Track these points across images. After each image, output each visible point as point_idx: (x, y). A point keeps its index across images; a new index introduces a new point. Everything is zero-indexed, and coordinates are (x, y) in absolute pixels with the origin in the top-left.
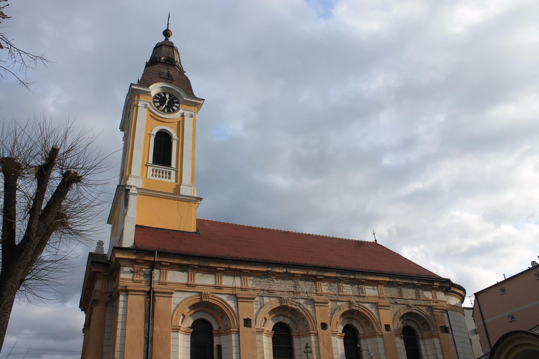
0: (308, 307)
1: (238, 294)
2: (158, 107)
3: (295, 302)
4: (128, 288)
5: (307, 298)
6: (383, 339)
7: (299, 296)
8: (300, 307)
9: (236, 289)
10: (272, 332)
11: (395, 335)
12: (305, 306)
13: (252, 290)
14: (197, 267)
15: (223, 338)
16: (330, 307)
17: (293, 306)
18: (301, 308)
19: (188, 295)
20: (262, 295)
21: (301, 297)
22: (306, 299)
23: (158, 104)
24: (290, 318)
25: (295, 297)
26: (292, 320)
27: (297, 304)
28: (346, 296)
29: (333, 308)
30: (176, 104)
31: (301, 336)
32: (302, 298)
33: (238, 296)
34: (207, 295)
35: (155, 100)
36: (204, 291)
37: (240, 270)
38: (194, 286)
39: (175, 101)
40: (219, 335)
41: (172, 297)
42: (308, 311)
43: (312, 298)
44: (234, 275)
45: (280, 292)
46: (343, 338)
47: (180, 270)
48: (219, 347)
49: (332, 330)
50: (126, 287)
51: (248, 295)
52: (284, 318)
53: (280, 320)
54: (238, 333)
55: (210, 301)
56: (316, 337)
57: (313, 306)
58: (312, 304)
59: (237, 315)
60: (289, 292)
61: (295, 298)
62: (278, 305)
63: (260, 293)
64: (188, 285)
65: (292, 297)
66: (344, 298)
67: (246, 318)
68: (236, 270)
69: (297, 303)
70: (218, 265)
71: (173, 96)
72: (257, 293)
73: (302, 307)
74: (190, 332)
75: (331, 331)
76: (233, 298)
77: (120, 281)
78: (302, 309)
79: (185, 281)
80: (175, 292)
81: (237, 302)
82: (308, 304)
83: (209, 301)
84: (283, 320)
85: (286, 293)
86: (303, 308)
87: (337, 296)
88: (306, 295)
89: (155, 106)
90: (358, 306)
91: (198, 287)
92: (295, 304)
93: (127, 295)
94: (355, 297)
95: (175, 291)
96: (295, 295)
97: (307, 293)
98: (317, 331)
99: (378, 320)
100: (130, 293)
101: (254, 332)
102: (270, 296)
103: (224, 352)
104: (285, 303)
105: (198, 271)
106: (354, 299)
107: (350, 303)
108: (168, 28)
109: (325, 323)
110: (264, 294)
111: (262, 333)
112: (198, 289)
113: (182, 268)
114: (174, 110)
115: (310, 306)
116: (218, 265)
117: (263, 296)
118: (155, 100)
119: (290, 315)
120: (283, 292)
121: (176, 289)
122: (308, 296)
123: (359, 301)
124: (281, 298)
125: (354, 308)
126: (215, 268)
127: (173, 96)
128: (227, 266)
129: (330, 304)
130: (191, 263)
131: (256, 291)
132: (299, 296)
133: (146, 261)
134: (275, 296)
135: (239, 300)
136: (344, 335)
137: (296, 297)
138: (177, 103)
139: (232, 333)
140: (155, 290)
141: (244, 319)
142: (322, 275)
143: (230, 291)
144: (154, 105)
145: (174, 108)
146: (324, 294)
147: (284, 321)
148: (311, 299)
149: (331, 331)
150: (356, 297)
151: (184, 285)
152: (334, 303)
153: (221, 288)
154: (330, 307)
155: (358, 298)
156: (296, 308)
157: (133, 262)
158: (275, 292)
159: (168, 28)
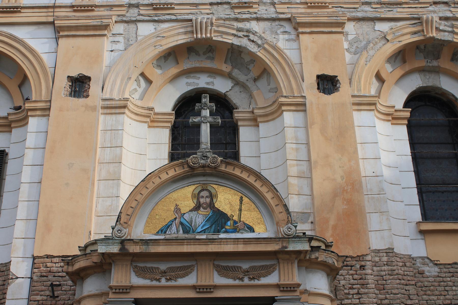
0: (278, 40)
3: (234, 29)
5: (274, 16)
7: (250, 13)
8: (250, 40)
9: (56, 10)
12: (269, 37)
13: (102, 9)
16: (350, 37)
17: (236, 41)
18: (253, 41)
20: (134, 19)
21: (254, 16)
22: (273, 20)
24: (229, 76)
25: (233, 16)
26: (237, 83)
27: (240, 34)
28: (404, 6)
29: (361, 38)
32: (258, 19)
42: (275, 48)
43: (289, 16)
45: (188, 7)
46: (406, 122)
49: (356, 93)
52: (210, 80)
53: (198, 84)
56: (301, 114)
57: (293, 37)
58: (293, 32)
60: (215, 7)
61: (237, 20)
62: (182, 39)
63: (128, 15)
65: (228, 16)
66: (399, 10)
67: (74, 74)
69: (239, 30)
72: (119, 16)
73: (255, 39)
75: (353, 96)
76: (48, 32)
78: (259, 46)
81: (57, 39)
82: (279, 32)
84: (208, 83)
85: (206, 9)
86: (260, 42)
87: (374, 6)
88: (273, 9)
90: (450, 29)
92: (234, 32)
94: (438, 6)
96: (237, 11)
97: (273, 4)
98: (304, 97)
101: (94, 109)
102: (156, 18)
104: (201, 34)
106: (434, 12)
107: (418, 20)
109: (331, 74)
110: (139, 15)
111: (122, 110)
115: (286, 36)
117: (136, 22)
119: (226, 68)
120: (196, 5)
122: (277, 12)
123: (450, 15)
124: (191, 20)
125: (434, 34)
129: (350, 27)
131: (115, 9)
132: (250, 13)
134: (173, 17)
136: (407, 115)
137: (239, 16)
141: (68, 77)
143: (41, 17)
146: (330, 3)
147: (210, 87)
148: (289, 20)
149: (353, 96)
150: (443, 5)
152: (366, 27)
154: (350, 37)
155: (447, 8)
156: (239, 44)
158: (173, 8)
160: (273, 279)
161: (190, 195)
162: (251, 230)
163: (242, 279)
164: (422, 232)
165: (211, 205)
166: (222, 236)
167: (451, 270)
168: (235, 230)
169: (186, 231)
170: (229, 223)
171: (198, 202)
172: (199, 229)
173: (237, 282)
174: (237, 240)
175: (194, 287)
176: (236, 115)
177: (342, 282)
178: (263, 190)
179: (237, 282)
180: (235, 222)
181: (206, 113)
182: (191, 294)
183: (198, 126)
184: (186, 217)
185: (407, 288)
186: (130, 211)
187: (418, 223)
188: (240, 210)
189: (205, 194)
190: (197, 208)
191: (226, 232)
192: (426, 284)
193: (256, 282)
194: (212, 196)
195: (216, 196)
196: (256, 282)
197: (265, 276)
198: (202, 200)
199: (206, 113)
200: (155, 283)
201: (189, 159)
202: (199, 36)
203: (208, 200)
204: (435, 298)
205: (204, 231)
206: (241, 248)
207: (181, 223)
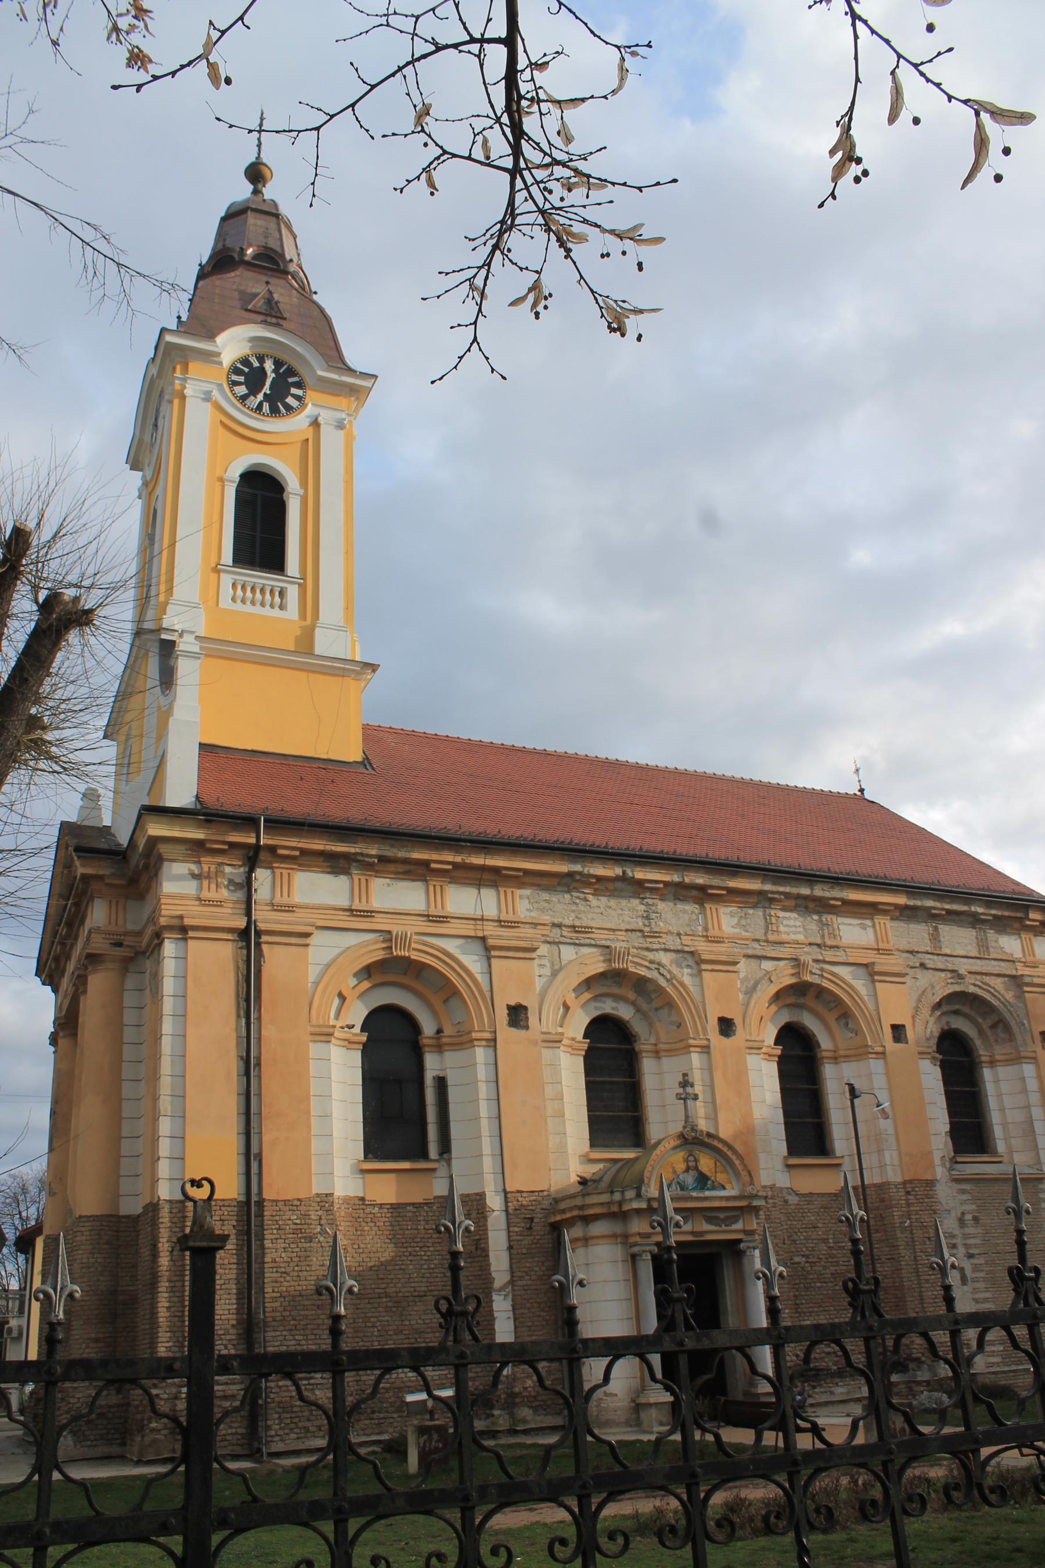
0: (683, 975)
1: (491, 935)
2: (243, 399)
3: (646, 960)
4: (187, 922)
5: (679, 948)
6: (886, 1063)
7: (659, 943)
8: (660, 973)
9: (485, 923)
10: (585, 1043)
11: (920, 1053)
12: (675, 970)
13: (527, 926)
14: (376, 861)
15: (451, 1058)
16: (742, 975)
17: (643, 972)
18: (663, 975)
19: (351, 939)
20: (557, 940)
21: (663, 946)
22: (677, 951)
23: (242, 390)
24: (633, 1004)
25: (645, 945)
26: (638, 1010)
27: (653, 966)
28: (786, 945)
29: (750, 976)
30: (294, 391)
31: (662, 1054)
32: (665, 950)
33: (491, 942)
35: (235, 378)
36: (395, 929)
37: (496, 870)
38: (369, 914)
39: (291, 380)
40: (439, 1048)
41: (307, 945)
42: (682, 984)
43: (692, 949)
44: (479, 884)
45: (606, 932)
46: (777, 1059)
47: (329, 870)
48: (441, 1083)
49: (748, 1038)
50: (181, 917)
51: (519, 938)
52: (614, 1005)
53: (604, 1009)
54: (492, 1044)
55: (415, 956)
56: (705, 1056)
57: (695, 971)
58: (695, 967)
59: (488, 995)
60: (630, 933)
61: (648, 949)
62: (601, 967)
63: (551, 935)
65: (640, 945)
66: (782, 949)
67: (512, 1003)
68: (483, 868)
69: (651, 962)
70: (435, 856)
71: (285, 367)
72: (543, 935)
73: (665, 973)
74: (359, 1043)
75: (747, 1040)
76: (477, 946)
77: (163, 901)
78: (668, 981)
79: (345, 903)
80: (316, 932)
81: (489, 958)
82: (683, 965)
83: (412, 957)
84: (613, 1008)
85: (622, 936)
86: (668, 977)
87: (762, 944)
88: (678, 940)
89: (234, 394)
90: (820, 973)
91: (379, 918)
92: (647, 964)
93: (185, 939)
94: (812, 947)
96: (648, 940)
97: (679, 935)
98: (708, 1040)
99: (874, 1013)
100: (191, 934)
101: (535, 1043)
102: (577, 942)
103: (453, 1095)
105: (379, 874)
106: (808, 953)
107: (796, 962)
108: (258, 157)
109: (729, 1017)
110: (562, 936)
111: (557, 1045)
112: (381, 923)
113: (336, 864)
114: (289, 408)
115: (689, 970)
116: (435, 856)
117: (558, 943)
118: (235, 378)
119: (631, 995)
120: (614, 930)
121: (320, 923)
122: (682, 944)
123: (821, 958)
124: (608, 947)
125: (808, 978)
126: (426, 864)
127: (285, 367)
128: (458, 859)
129: (742, 966)
130: (358, 850)
131: (539, 927)
132: (659, 943)
133: (232, 845)
134: (593, 942)
135: (493, 953)
136: (779, 1052)
137: (648, 945)
138: (299, 385)
139: (476, 1043)
140: (262, 926)
141: (507, 1005)
142: (722, 885)
143: (468, 929)
144: (232, 391)
145: (290, 400)
146: (727, 938)
147: (615, 1012)
148: (692, 953)
149: (747, 1040)
150: (815, 947)
151: (341, 913)
152: (754, 962)
153: (442, 919)
154: (742, 975)
155: (818, 950)
156: (650, 977)
158: (593, 932)
159: (258, 157)
160: (739, 1226)
161: (681, 1160)
162: (724, 1188)
164: (789, 1166)
165: (696, 1168)
166: (707, 1193)
167: (807, 1199)
168: (714, 1188)
169: (682, 1189)
170: (709, 1182)
171: (688, 1165)
172: (690, 1188)
174: (721, 1198)
175: (692, 1233)
178: (734, 1157)
179: (718, 1228)
180: (713, 1182)
182: (690, 1238)
184: (681, 1177)
187: (784, 1157)
188: (716, 1172)
189: (691, 1158)
190: (687, 1170)
191: (708, 1189)
192: (790, 1211)
193: (729, 1228)
194: (696, 1161)
195: (699, 1161)
196: (729, 1228)
197: (734, 1223)
198: (690, 1164)
203: (694, 1164)
204: (795, 1223)
205: (693, 1189)
206: (724, 1204)
207: (678, 1183)
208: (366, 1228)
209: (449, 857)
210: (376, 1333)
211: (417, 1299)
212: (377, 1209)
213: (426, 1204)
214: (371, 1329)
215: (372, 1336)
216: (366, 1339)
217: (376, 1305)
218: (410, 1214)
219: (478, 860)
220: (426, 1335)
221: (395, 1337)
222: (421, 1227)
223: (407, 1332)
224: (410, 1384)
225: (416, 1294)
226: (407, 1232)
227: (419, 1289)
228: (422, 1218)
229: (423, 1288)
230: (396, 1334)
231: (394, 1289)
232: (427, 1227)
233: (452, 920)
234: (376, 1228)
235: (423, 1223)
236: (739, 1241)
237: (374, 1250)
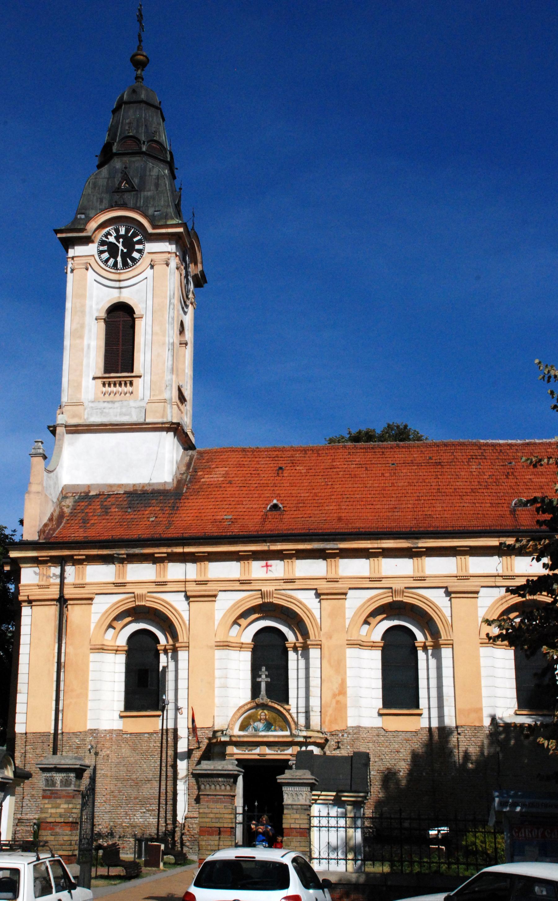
2: (107, 261)
4: (31, 598)
11: (481, 643)
23: (106, 255)
30: (137, 247)
33: (189, 594)
34: (141, 597)
35: (102, 248)
37: (193, 554)
38: (123, 584)
39: (135, 240)
41: (92, 604)
46: (381, 648)
49: (349, 639)
50: (28, 596)
51: (205, 591)
55: (148, 604)
59: (187, 622)
64: (116, 585)
68: (184, 554)
77: (20, 588)
79: (112, 580)
83: (147, 605)
91: (128, 586)
93: (32, 606)
95: (97, 594)
99: (449, 619)
100: (34, 603)
114: (134, 260)
118: (102, 248)
128: (169, 550)
130: (114, 552)
135: (191, 599)
136: (382, 644)
138: (140, 242)
140: (67, 597)
142: (335, 547)
145: (135, 255)
153: (164, 583)
157: (35, 561)
163: (277, 751)
166: (270, 733)
167: (394, 734)
168: (275, 730)
169: (256, 730)
173: (275, 752)
175: (258, 755)
176: (287, 645)
177: (332, 743)
181: (263, 676)
183: (260, 682)
185: (368, 744)
186: (233, 722)
189: (263, 714)
191: (272, 731)
193: (283, 753)
196: (283, 753)
198: (262, 717)
199: (263, 676)
200: (243, 752)
201: (256, 700)
202: (266, 601)
204: (383, 748)
205: (263, 731)
206: (276, 739)
207: (254, 727)
208: (123, 745)
209: (164, 550)
210: (124, 798)
211: (147, 782)
212: (129, 736)
213: (155, 733)
214: (122, 796)
215: (123, 799)
216: (119, 801)
217: (125, 784)
218: (146, 738)
219: (179, 550)
220: (151, 801)
221: (134, 801)
222: (151, 745)
223: (140, 798)
224: (140, 825)
225: (146, 779)
226: (144, 747)
227: (148, 777)
228: (152, 740)
229: (151, 777)
230: (135, 799)
231: (135, 777)
232: (155, 745)
233: (169, 583)
234: (127, 745)
235: (153, 743)
236: (289, 760)
237: (126, 756)
